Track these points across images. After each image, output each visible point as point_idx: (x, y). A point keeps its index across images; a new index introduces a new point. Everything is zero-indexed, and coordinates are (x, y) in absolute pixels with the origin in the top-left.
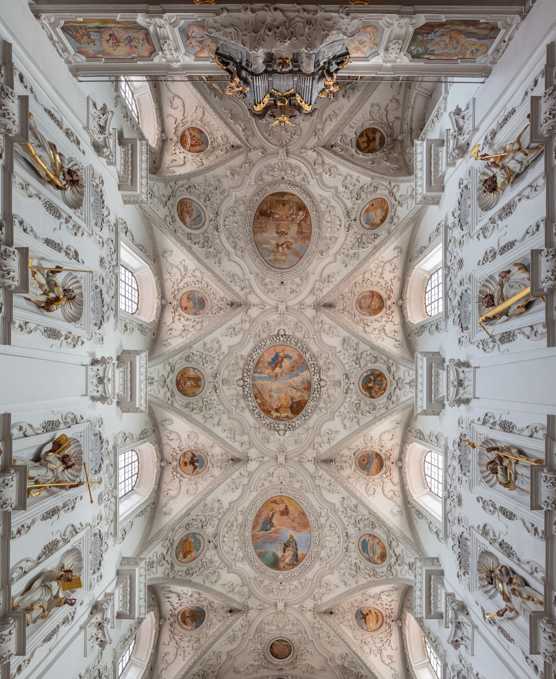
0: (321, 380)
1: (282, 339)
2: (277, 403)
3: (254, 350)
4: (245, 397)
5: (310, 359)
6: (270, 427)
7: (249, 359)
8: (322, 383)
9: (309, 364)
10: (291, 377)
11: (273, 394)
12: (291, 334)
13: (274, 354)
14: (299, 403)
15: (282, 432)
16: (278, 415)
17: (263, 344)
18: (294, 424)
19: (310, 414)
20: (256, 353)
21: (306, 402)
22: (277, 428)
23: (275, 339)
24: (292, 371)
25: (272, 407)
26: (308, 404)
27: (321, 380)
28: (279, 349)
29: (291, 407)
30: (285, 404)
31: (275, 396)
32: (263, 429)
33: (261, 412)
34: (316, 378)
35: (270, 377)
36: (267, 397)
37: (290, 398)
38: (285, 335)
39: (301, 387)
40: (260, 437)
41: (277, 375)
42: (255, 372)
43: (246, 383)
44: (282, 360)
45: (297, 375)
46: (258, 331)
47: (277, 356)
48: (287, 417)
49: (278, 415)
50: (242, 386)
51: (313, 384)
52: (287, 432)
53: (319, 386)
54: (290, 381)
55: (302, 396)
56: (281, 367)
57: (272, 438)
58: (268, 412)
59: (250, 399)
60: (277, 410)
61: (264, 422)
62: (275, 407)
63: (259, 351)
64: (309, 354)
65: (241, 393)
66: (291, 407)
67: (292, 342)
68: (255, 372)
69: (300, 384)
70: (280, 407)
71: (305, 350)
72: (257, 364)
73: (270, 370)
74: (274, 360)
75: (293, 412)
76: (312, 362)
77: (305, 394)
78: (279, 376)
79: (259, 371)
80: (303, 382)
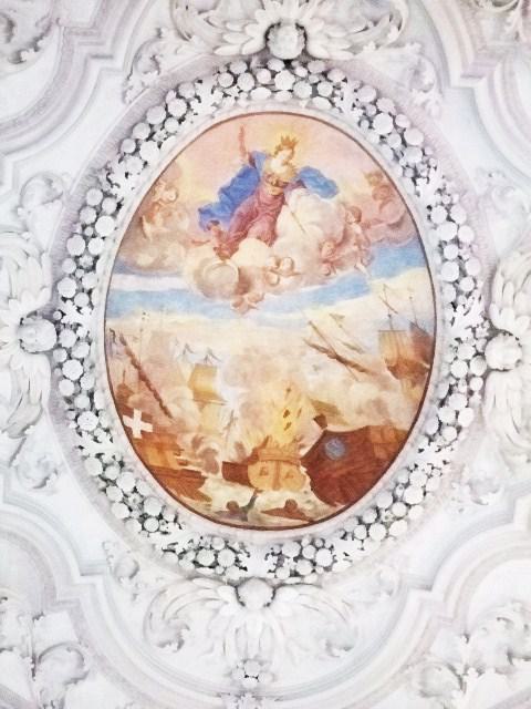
0: (494, 332)
1: (284, 80)
2: (237, 434)
3: (126, 144)
4: (67, 409)
5: (439, 214)
6: (196, 563)
7: (95, 197)
8: (498, 353)
9: (431, 244)
10: (321, 299)
11: (218, 385)
12: (338, 53)
13: (238, 164)
14: (358, 440)
15: (256, 594)
16: (242, 496)
17: (178, 108)
18: (323, 558)
19: (414, 513)
20: (133, 164)
21: (402, 439)
22: (236, 574)
23: (246, 82)
24: (333, 264)
25: (209, 453)
26: (408, 455)
27: (494, 332)
28: (263, 138)
29: (315, 462)
30: (282, 439)
31: (231, 396)
32: (152, 574)
33: (149, 486)
34: (467, 319)
35: (207, 291)
36: (181, 403)
37: (310, 413)
38: (306, 57)
39: (376, 354)
40: (134, 615)
41: (244, 285)
42: (120, 268)
43: (68, 338)
44: (281, 199)
45: (360, 289)
46: (147, 31)
47: (251, 171)
48: (290, 509)
49: (242, 496)
50: (49, 354)
51: (443, 354)
52: (285, 595)
53: (477, 368)
54: (320, 315)
55: (379, 405)
56: (271, 237)
57: (199, 618)
58: (182, 482)
59: (88, 421)
60: (236, 473)
61: (164, 542)
62: (226, 454)
63: (148, 150)
64: (436, 181)
65: (43, 386)
66: (315, 462)
67: (346, 105)
68: (120, 268)
69: (370, 341)
70: (255, 458)
71: (414, 158)
72: (137, 222)
73: (208, 252)
74: (231, 195)
75: (320, 487)
76: (447, 232)
77: (397, 401)
78: (258, 288)
79: (144, 259)
80: (388, 333)
